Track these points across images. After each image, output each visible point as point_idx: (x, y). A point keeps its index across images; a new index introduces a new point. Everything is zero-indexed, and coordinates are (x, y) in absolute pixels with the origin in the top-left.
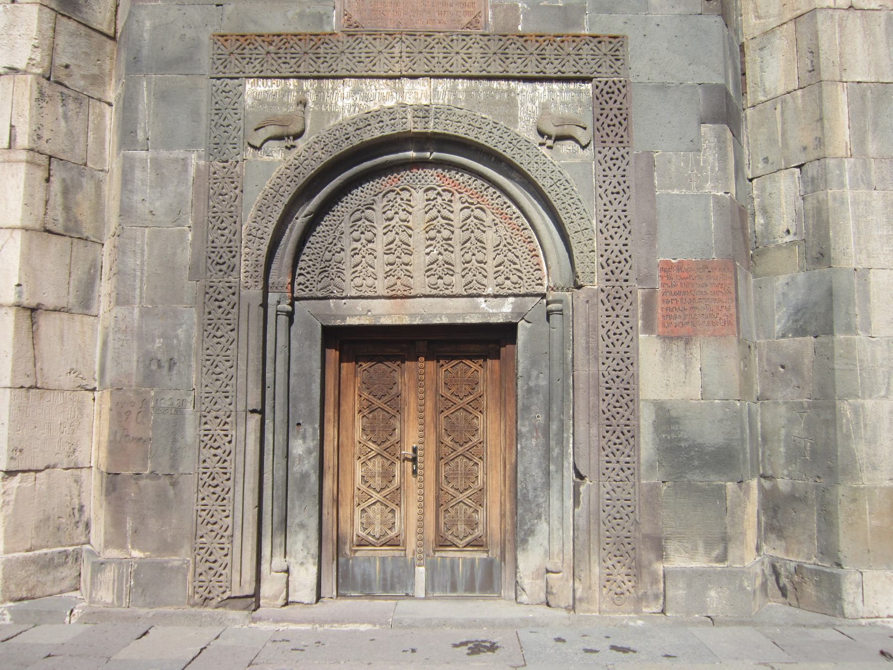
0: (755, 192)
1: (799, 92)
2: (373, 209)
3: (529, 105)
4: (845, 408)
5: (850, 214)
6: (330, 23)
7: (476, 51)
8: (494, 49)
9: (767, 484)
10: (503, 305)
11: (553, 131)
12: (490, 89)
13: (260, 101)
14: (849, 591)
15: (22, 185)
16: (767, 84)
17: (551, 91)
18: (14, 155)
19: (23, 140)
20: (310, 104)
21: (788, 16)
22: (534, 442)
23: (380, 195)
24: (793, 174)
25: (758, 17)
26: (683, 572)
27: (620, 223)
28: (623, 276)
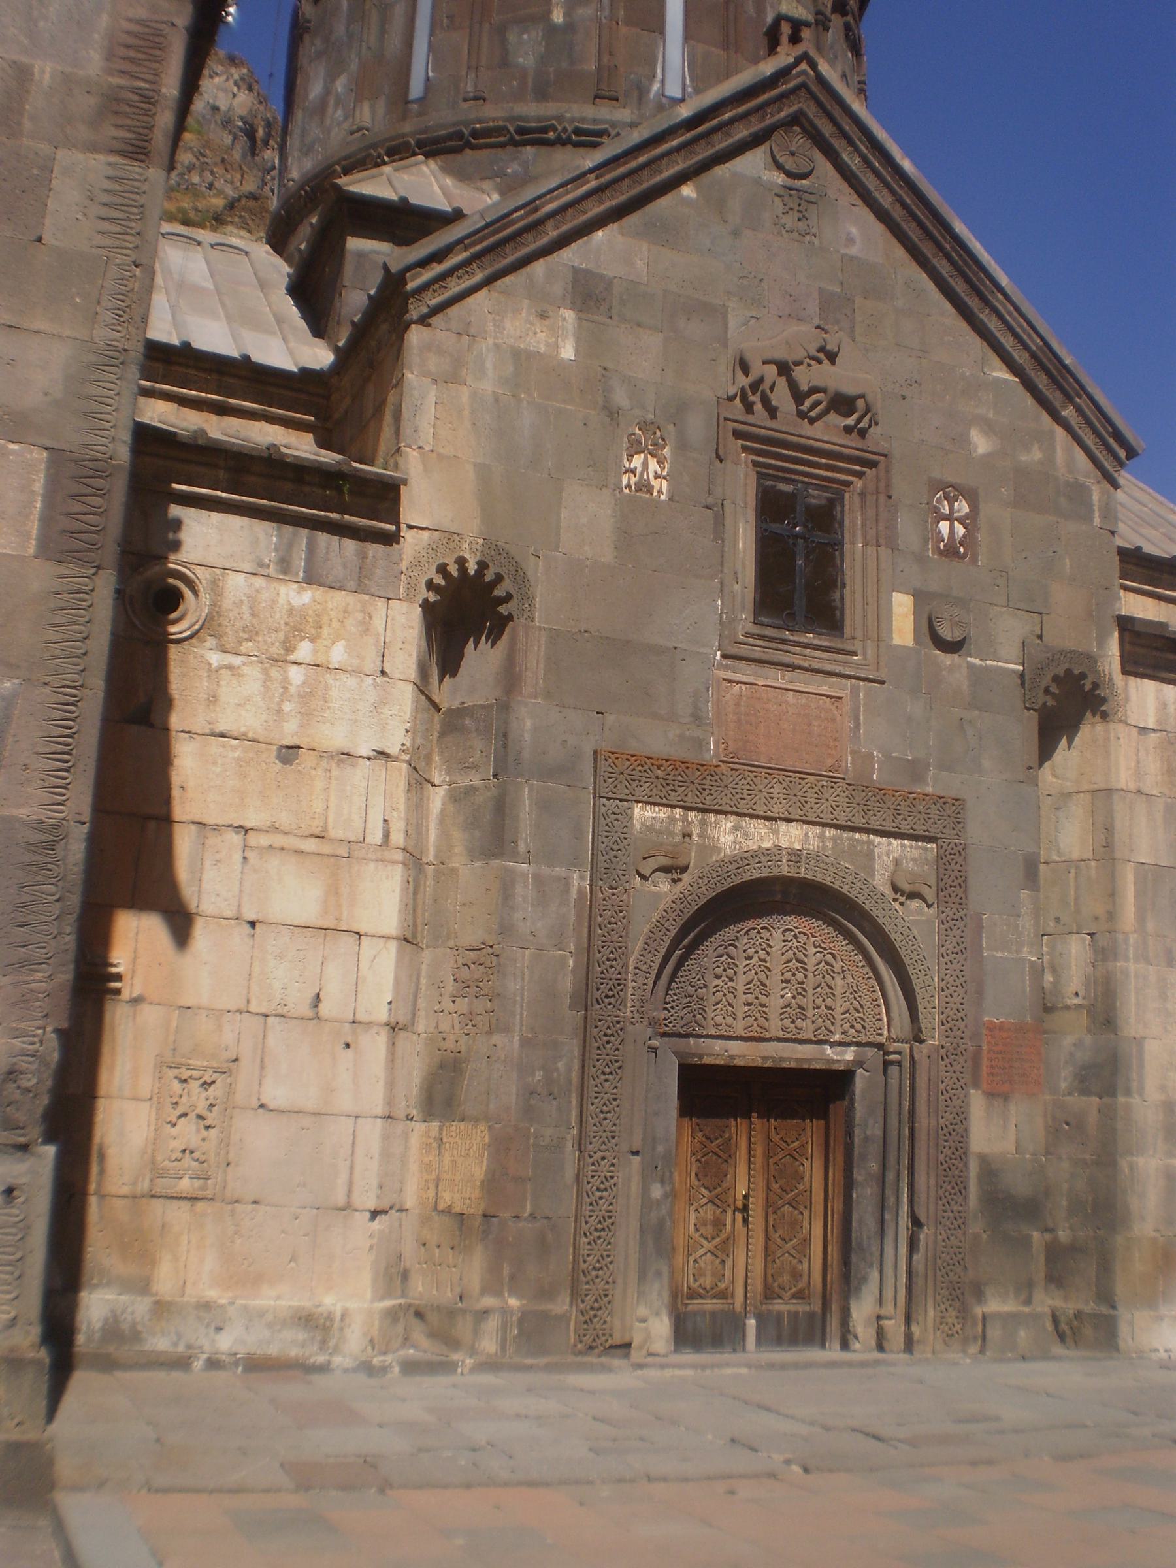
0: (1045, 949)
1: (1093, 863)
2: (735, 947)
3: (885, 858)
4: (1123, 1164)
5: (1132, 987)
6: (709, 750)
7: (842, 800)
8: (858, 799)
9: (1047, 1236)
10: (845, 1053)
11: (907, 887)
12: (852, 839)
13: (648, 828)
14: (1123, 1330)
15: (398, 890)
16: (1062, 846)
17: (903, 846)
18: (388, 855)
19: (398, 838)
20: (694, 836)
21: (1086, 787)
22: (869, 1191)
23: (742, 933)
24: (1084, 940)
25: (1055, 776)
26: (998, 1315)
27: (958, 982)
28: (959, 1033)
